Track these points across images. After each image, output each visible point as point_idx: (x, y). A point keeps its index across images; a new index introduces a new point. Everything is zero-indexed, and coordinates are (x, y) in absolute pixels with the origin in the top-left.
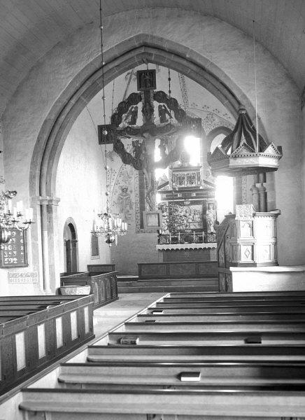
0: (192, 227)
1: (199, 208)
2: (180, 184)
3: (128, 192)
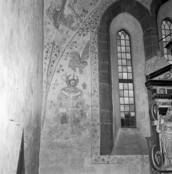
3: (79, 86)
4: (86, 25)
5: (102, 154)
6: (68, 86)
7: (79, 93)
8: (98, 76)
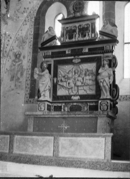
0: (82, 92)
1: (92, 66)
4: (28, 18)
5: (29, 98)
6: (15, 59)
7: (20, 62)
8: (32, 50)
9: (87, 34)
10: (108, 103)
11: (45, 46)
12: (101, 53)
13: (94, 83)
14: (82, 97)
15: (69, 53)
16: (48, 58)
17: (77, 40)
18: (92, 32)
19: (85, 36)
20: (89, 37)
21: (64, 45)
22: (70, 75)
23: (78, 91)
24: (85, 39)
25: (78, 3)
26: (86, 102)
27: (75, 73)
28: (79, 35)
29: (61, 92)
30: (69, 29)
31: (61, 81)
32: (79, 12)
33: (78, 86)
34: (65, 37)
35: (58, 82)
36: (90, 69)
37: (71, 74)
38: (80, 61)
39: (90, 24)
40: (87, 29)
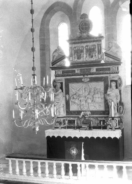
0: (92, 108)
1: (100, 85)
2: (78, 58)
9: (94, 54)
10: (116, 121)
11: (55, 66)
12: (107, 74)
13: (103, 101)
14: (93, 112)
15: (78, 72)
16: (60, 76)
17: (85, 60)
18: (98, 54)
19: (92, 57)
20: (96, 57)
21: (74, 65)
22: (81, 93)
23: (89, 107)
24: (92, 59)
25: (84, 24)
26: (97, 117)
27: (85, 91)
28: (86, 54)
29: (73, 108)
30: (77, 49)
31: (73, 98)
32: (85, 32)
33: (89, 103)
34: (73, 56)
35: (70, 99)
36: (97, 87)
37: (82, 92)
38: (89, 80)
39: (96, 45)
40: (94, 50)
